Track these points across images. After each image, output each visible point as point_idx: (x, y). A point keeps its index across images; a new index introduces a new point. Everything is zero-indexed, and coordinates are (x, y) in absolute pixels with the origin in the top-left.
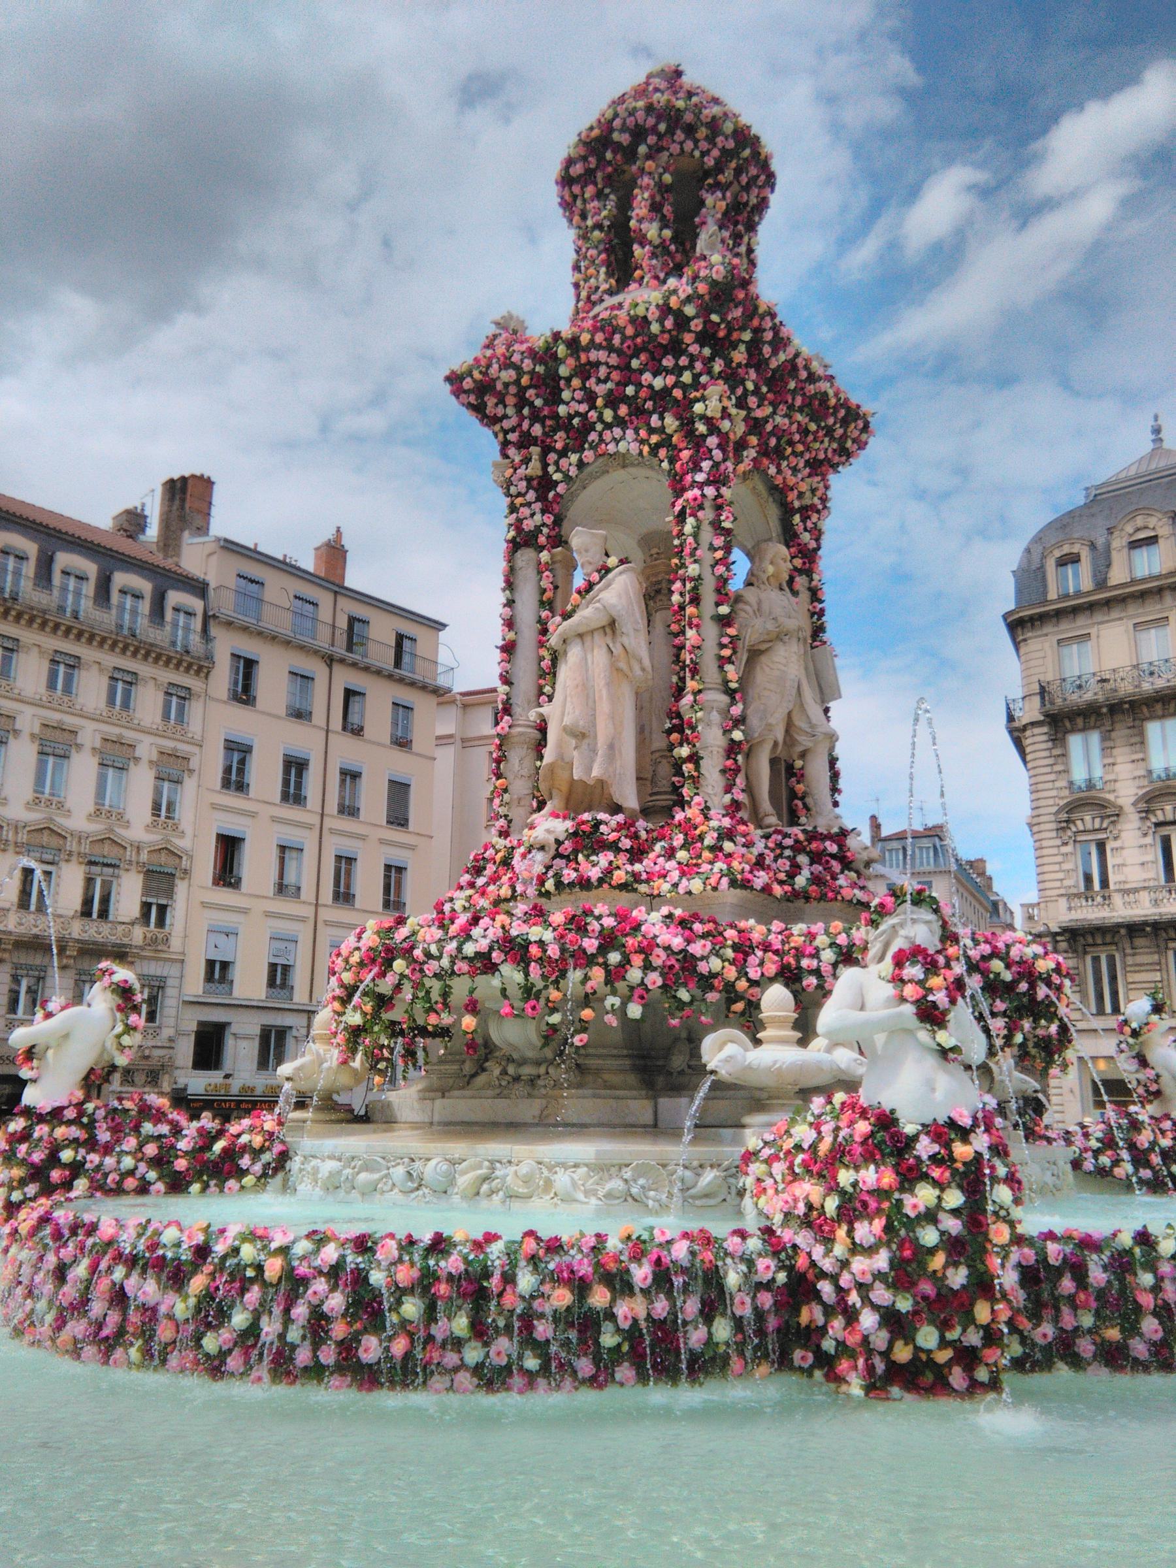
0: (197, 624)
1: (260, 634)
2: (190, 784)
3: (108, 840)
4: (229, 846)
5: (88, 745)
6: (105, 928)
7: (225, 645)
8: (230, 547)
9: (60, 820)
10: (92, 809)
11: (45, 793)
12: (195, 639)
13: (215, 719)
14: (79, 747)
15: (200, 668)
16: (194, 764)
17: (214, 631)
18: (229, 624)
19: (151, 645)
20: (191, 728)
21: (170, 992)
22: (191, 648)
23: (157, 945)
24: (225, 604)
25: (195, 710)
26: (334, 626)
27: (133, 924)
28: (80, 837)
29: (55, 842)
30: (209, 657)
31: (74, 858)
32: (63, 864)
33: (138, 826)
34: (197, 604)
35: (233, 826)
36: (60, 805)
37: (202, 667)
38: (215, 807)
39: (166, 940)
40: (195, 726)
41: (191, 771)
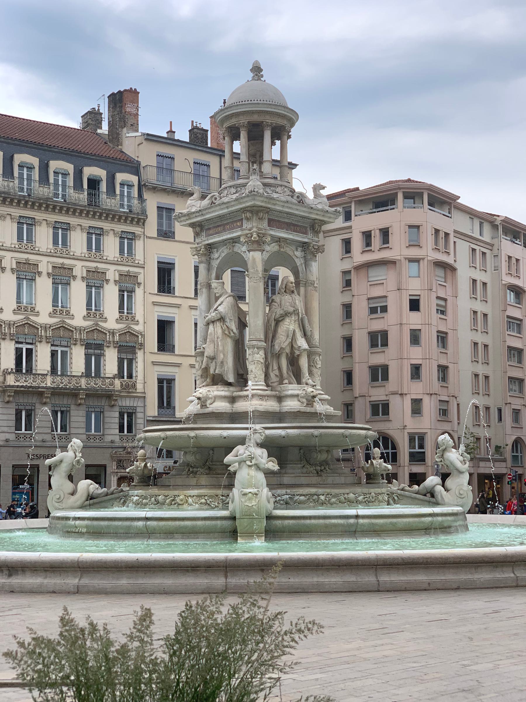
0: (135, 192)
1: (174, 192)
2: (139, 292)
3: (96, 330)
4: (164, 328)
5: (79, 276)
6: (99, 382)
7: (152, 202)
8: (150, 138)
9: (68, 321)
10: (85, 313)
11: (59, 307)
12: (135, 202)
13: (150, 251)
14: (74, 278)
15: (139, 220)
16: (140, 279)
17: (146, 195)
18: (154, 189)
19: (109, 210)
20: (137, 258)
21: (140, 415)
22: (134, 209)
23: (129, 388)
24: (151, 175)
25: (139, 245)
26: (221, 179)
27: (114, 378)
28: (80, 330)
29: (67, 334)
30: (144, 212)
31: (78, 343)
32: (73, 347)
33: (111, 320)
34: (134, 179)
35: (166, 313)
36: (68, 313)
37: (140, 220)
38: (155, 304)
39: (134, 386)
40: (139, 256)
41: (139, 284)
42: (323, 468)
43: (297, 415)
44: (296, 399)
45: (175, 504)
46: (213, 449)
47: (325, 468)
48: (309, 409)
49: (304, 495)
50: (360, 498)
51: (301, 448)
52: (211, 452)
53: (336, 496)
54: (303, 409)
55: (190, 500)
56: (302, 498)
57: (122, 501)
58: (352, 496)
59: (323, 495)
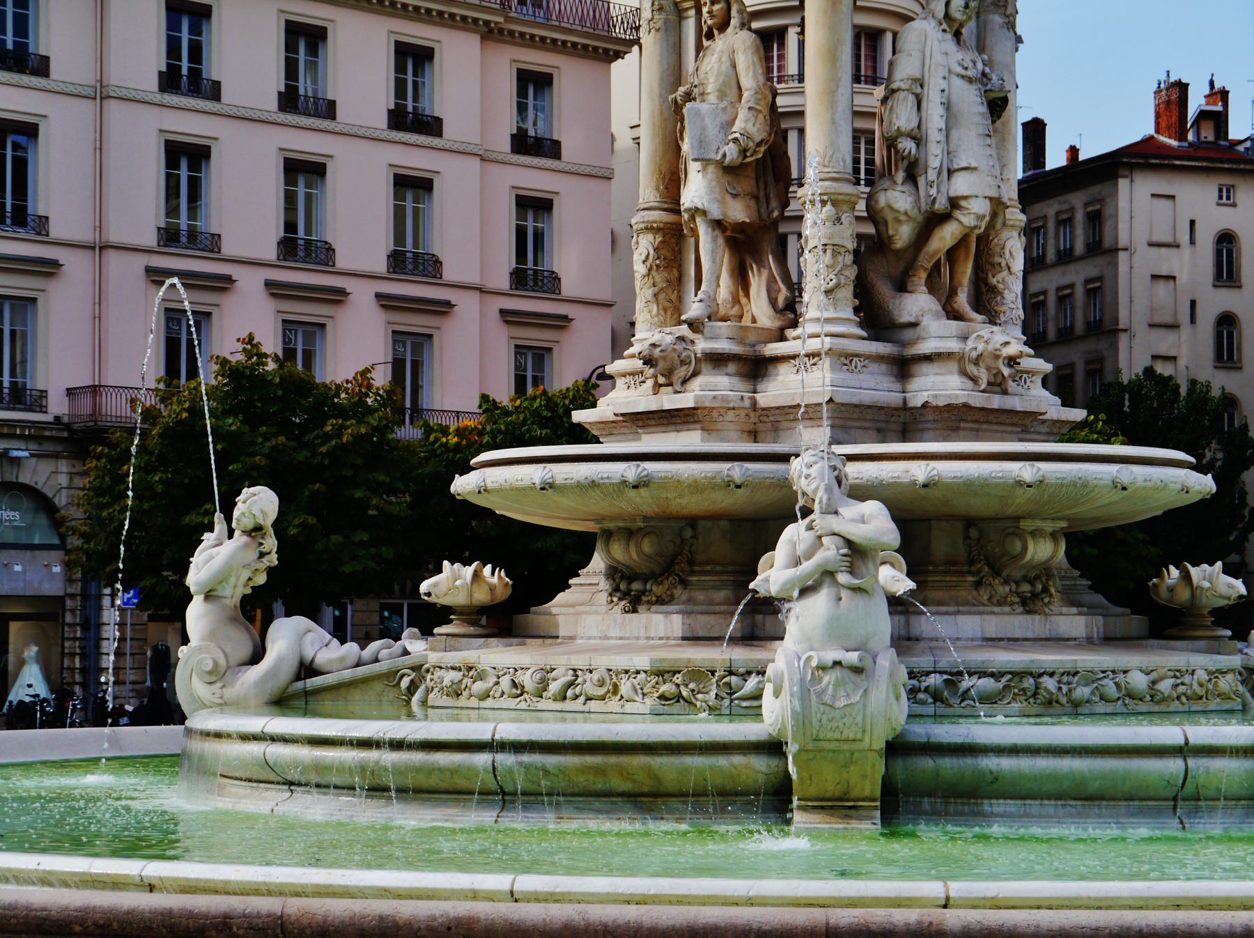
42: (1039, 587)
43: (956, 419)
44: (954, 366)
45: (576, 697)
46: (692, 521)
47: (1045, 590)
48: (996, 402)
49: (992, 675)
50: (1165, 686)
51: (970, 522)
52: (688, 533)
53: (1091, 677)
54: (978, 400)
55: (625, 688)
56: (986, 684)
57: (405, 683)
58: (1139, 681)
59: (1052, 675)
